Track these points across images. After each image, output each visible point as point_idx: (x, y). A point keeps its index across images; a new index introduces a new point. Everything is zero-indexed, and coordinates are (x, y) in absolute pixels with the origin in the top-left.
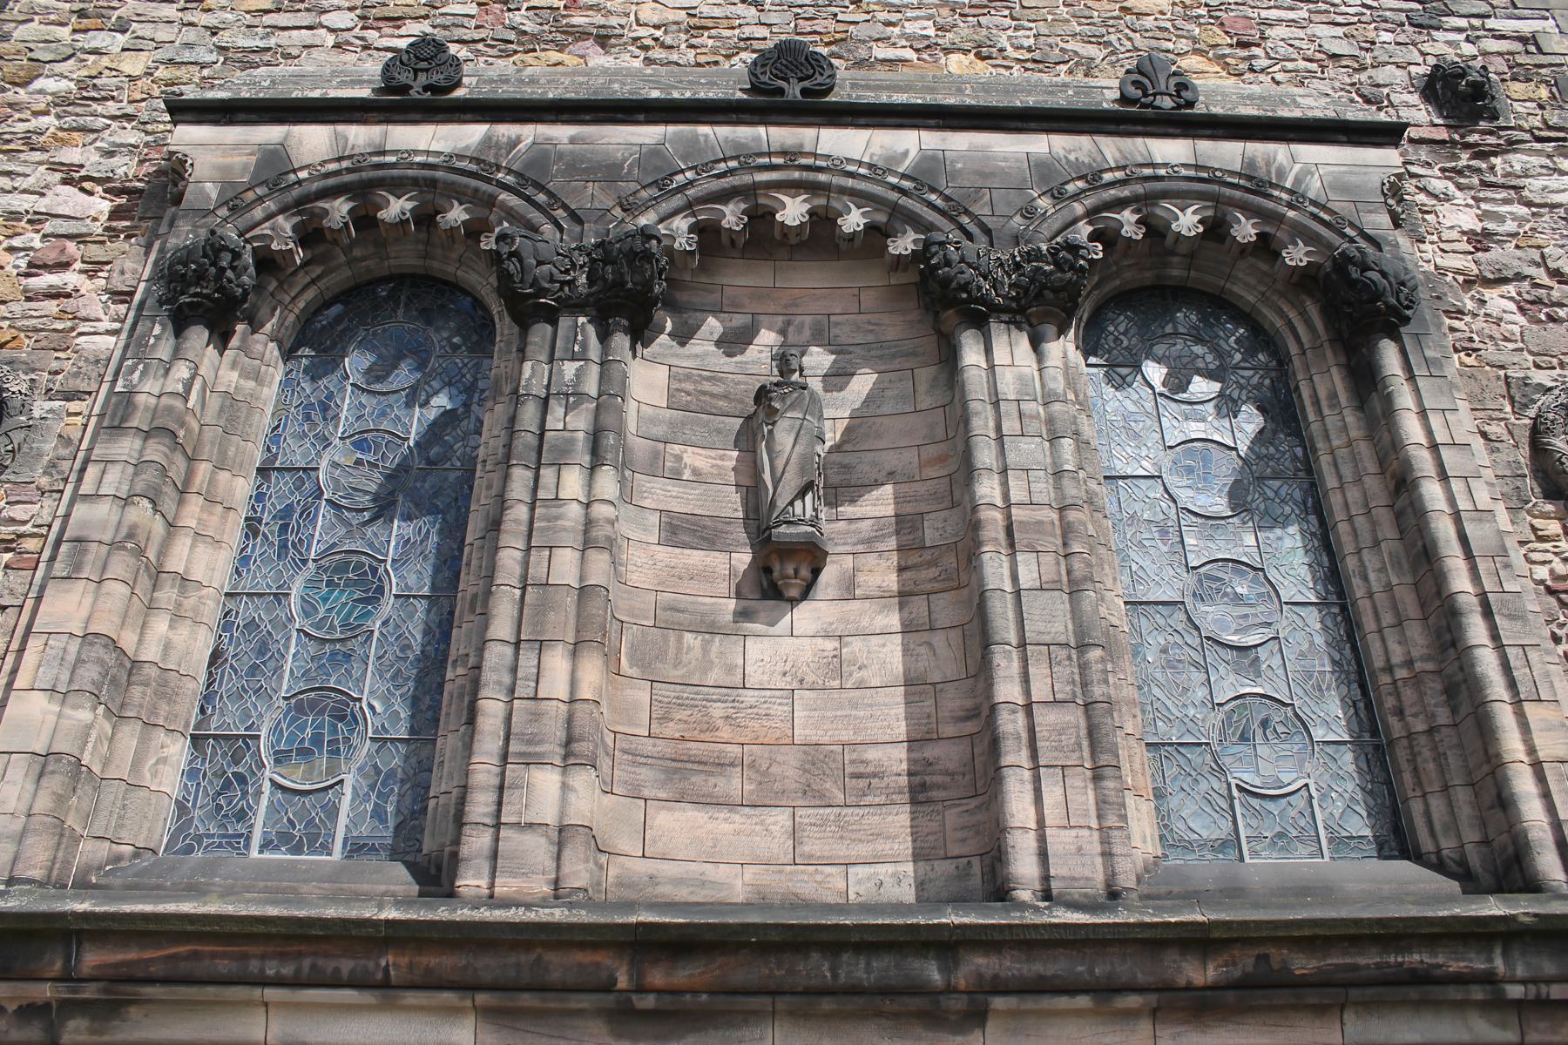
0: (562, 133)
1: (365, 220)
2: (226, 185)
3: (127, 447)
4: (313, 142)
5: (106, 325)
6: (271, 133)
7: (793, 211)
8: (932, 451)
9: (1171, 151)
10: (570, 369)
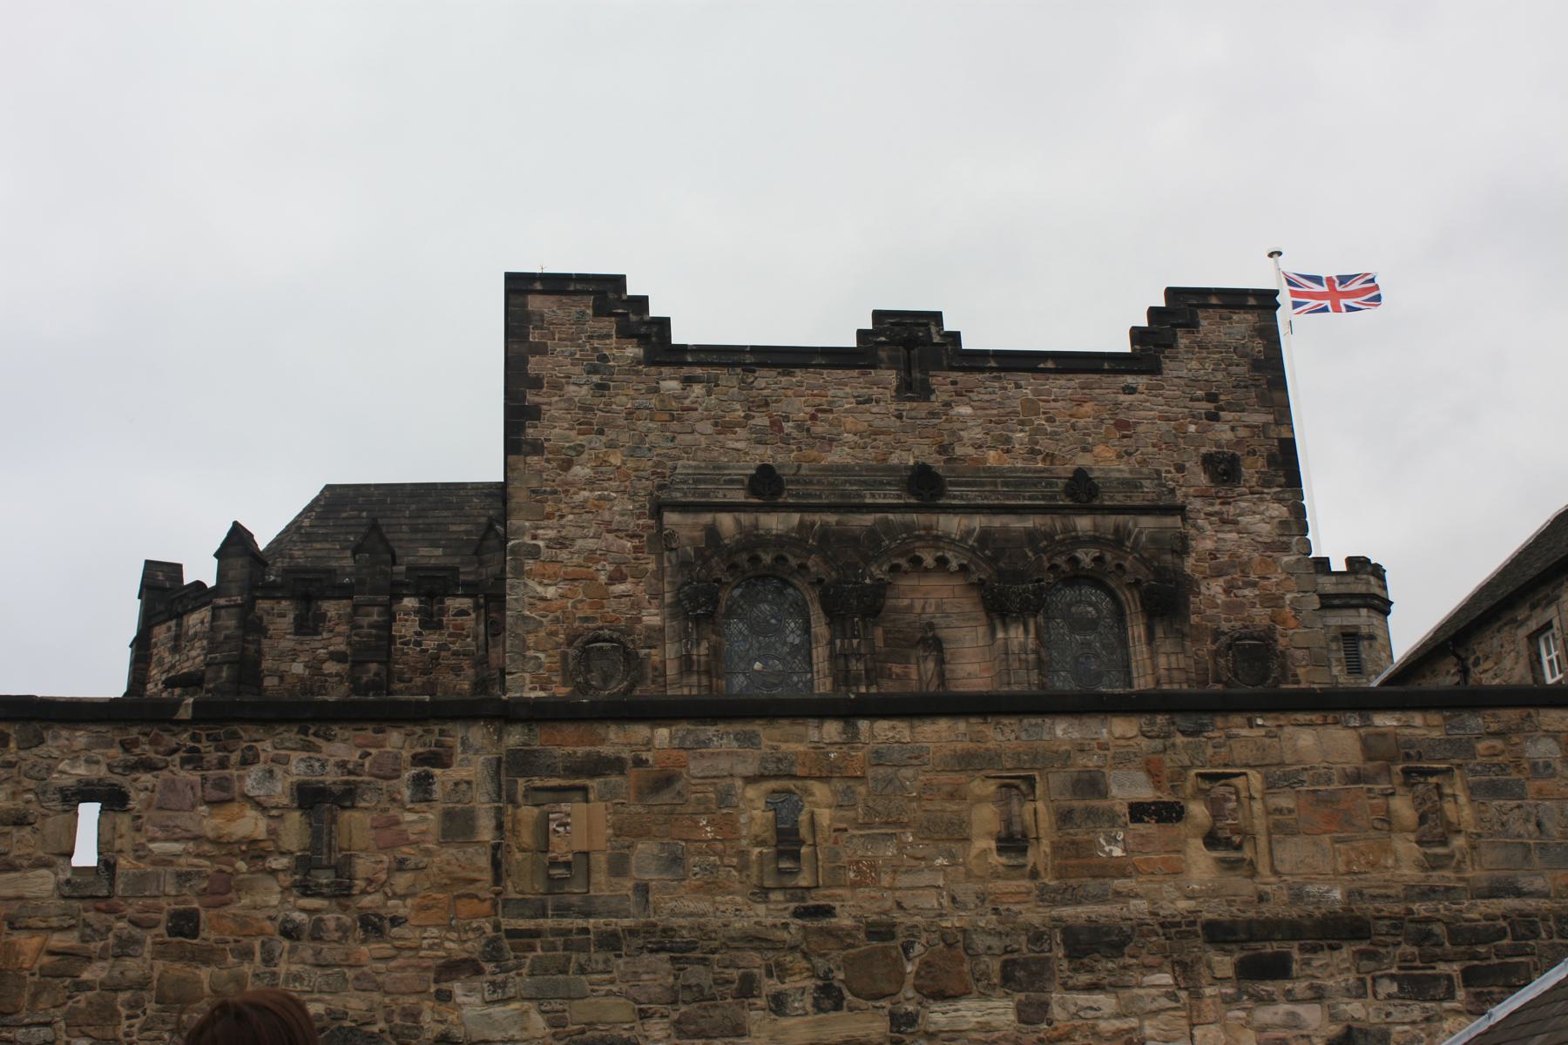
0: (832, 518)
1: (755, 559)
2: (697, 550)
3: (694, 679)
4: (726, 521)
5: (653, 611)
6: (707, 518)
7: (929, 559)
8: (984, 665)
9: (1084, 523)
10: (855, 642)
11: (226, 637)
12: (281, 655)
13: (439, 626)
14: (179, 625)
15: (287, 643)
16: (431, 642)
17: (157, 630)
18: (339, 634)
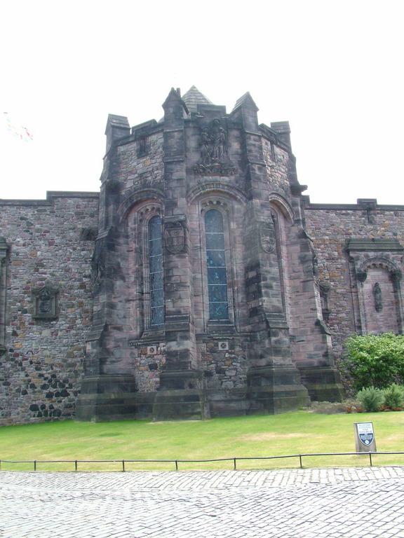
14: (272, 148)
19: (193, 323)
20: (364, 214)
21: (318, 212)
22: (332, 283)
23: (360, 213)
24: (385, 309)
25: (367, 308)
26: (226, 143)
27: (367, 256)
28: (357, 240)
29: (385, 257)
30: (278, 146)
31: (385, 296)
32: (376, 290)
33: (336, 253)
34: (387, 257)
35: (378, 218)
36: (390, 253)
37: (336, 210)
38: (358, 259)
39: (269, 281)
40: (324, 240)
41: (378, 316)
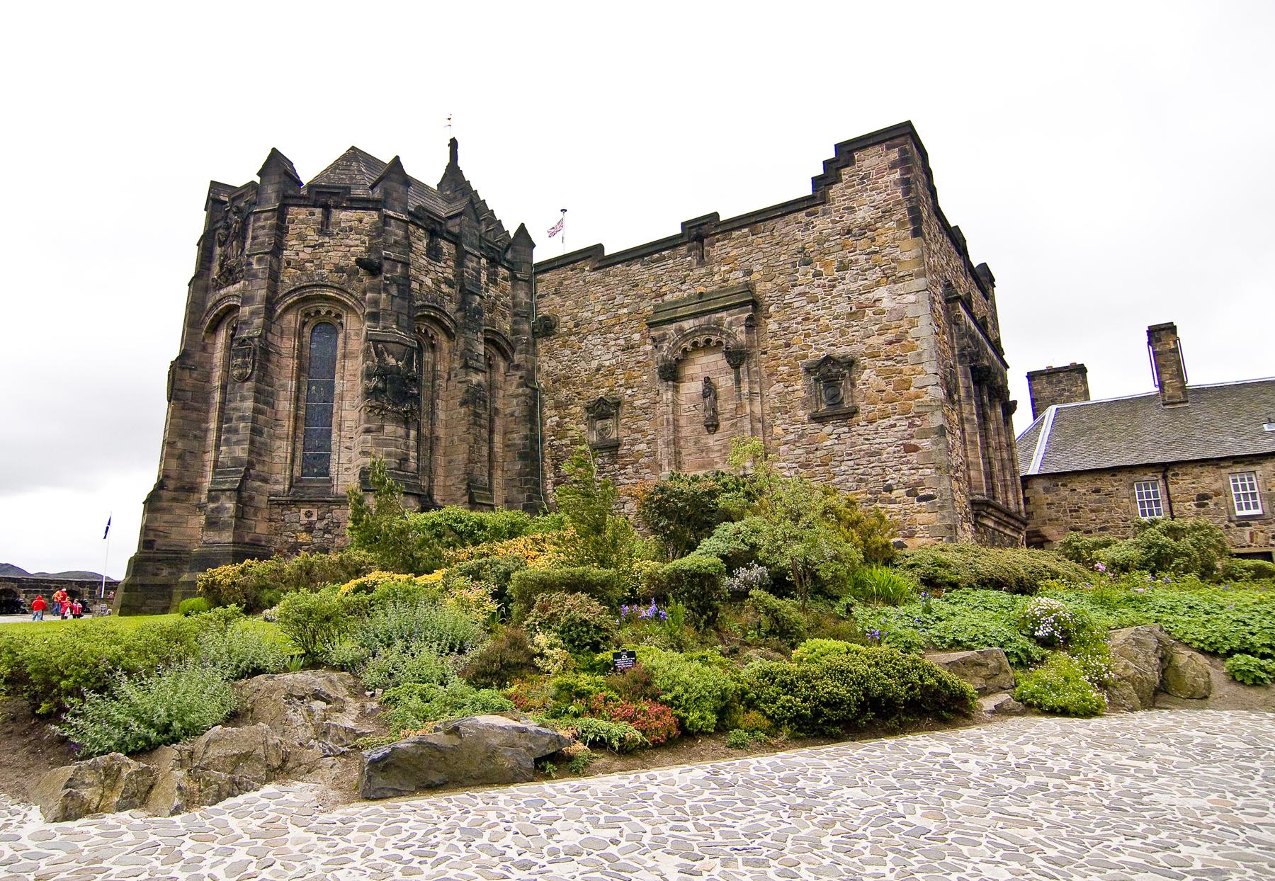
11: (396, 242)
12: (419, 269)
13: (495, 282)
15: (423, 261)
16: (493, 291)
17: (291, 209)
18: (449, 267)
19: (193, 489)
20: (689, 250)
21: (612, 270)
22: (629, 392)
23: (683, 250)
24: (724, 425)
25: (686, 432)
26: (241, 235)
27: (681, 330)
28: (676, 302)
29: (716, 323)
30: (346, 209)
31: (726, 400)
32: (709, 389)
33: (637, 336)
34: (719, 323)
35: (718, 249)
36: (724, 314)
37: (643, 256)
38: (663, 338)
39: (234, 423)
40: (618, 317)
41: (711, 440)
